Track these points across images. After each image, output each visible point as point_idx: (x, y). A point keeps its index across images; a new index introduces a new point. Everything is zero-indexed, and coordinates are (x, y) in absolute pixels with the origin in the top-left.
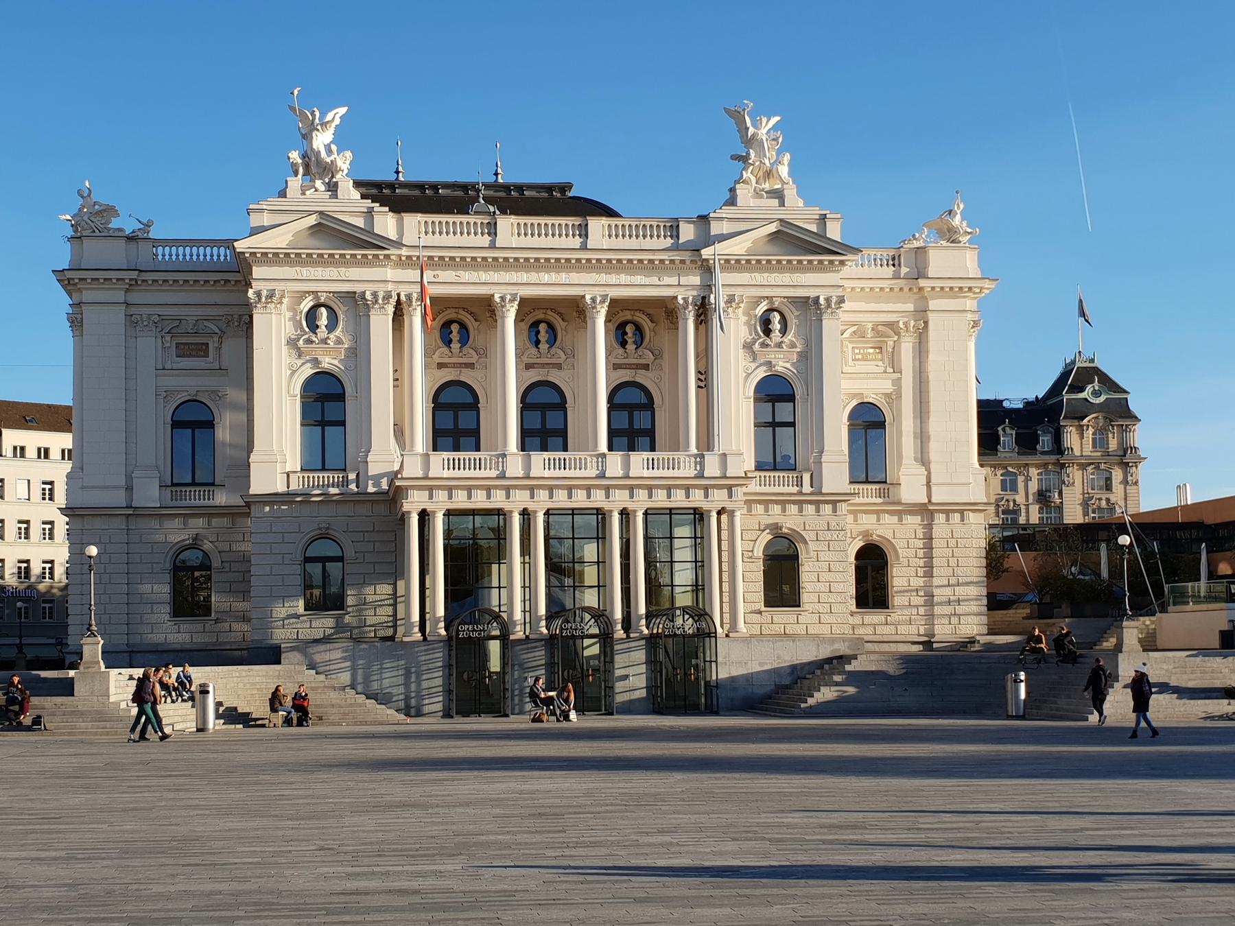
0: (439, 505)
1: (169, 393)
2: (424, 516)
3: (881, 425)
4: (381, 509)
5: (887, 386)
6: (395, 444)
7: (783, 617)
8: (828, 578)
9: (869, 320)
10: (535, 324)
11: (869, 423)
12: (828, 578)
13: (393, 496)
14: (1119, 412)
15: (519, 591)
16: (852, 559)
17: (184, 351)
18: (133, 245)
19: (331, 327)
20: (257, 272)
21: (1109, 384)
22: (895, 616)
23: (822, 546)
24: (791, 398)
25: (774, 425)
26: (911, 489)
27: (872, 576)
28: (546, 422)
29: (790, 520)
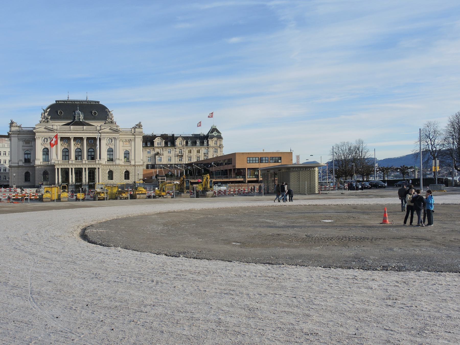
0: (60, 167)
1: (24, 149)
2: (58, 169)
5: (130, 148)
6: (56, 157)
9: (127, 139)
13: (54, 166)
14: (219, 137)
15: (72, 179)
16: (124, 173)
17: (26, 143)
19: (47, 142)
20: (36, 134)
21: (218, 132)
24: (113, 151)
26: (133, 163)
27: (127, 175)
29: (112, 168)
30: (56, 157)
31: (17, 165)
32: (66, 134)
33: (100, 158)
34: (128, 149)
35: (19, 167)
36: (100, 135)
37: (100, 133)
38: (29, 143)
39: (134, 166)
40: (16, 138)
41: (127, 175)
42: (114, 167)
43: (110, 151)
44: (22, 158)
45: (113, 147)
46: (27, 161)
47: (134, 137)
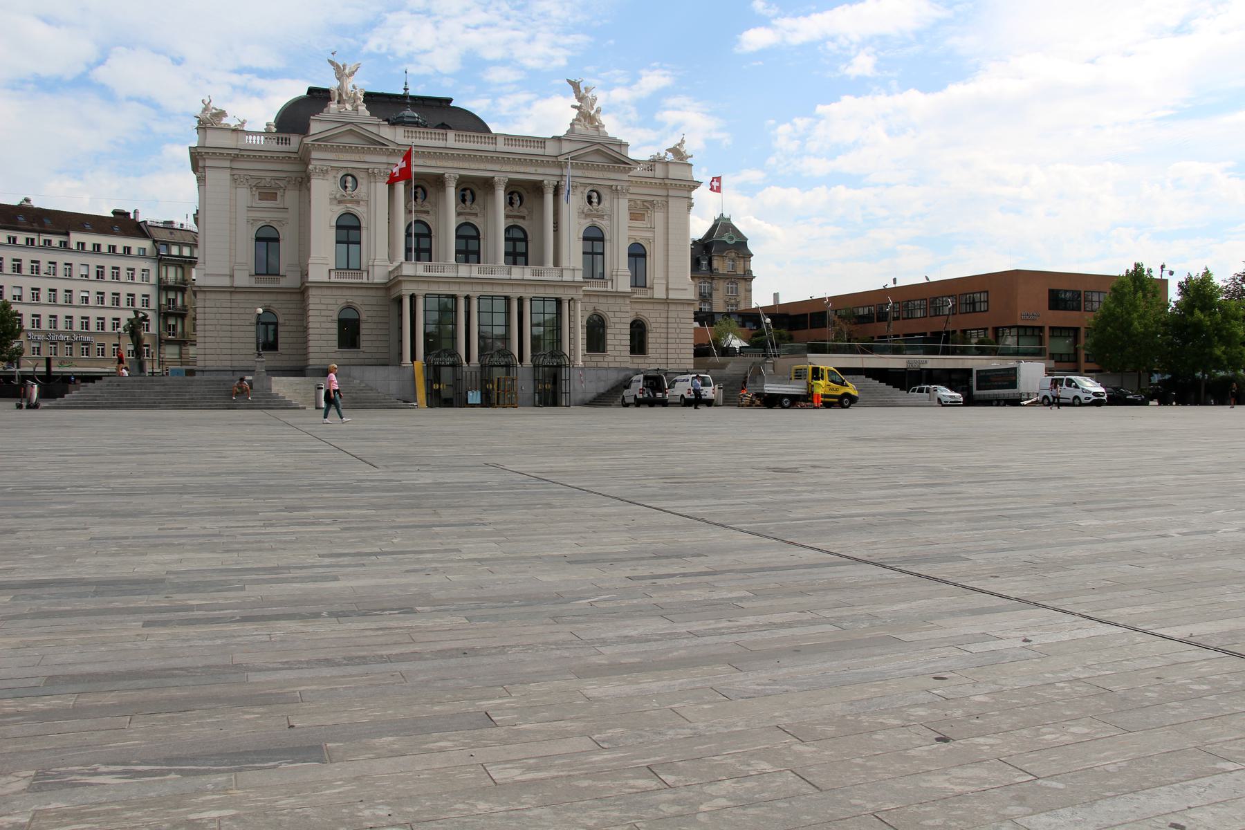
2: (413, 298)
3: (644, 256)
4: (381, 293)
7: (596, 357)
8: (619, 338)
10: (464, 190)
11: (637, 254)
12: (619, 338)
18: (234, 135)
20: (314, 155)
22: (648, 361)
23: (617, 320)
24: (602, 239)
25: (593, 253)
28: (469, 247)
30: (382, 253)
31: (226, 282)
32: (429, 163)
33: (557, 262)
34: (640, 236)
35: (233, 291)
36: (558, 172)
37: (560, 165)
38: (273, 197)
39: (667, 302)
40: (226, 175)
41: (638, 338)
42: (611, 300)
43: (594, 239)
44: (246, 251)
45: (603, 224)
46: (267, 268)
47: (664, 193)
